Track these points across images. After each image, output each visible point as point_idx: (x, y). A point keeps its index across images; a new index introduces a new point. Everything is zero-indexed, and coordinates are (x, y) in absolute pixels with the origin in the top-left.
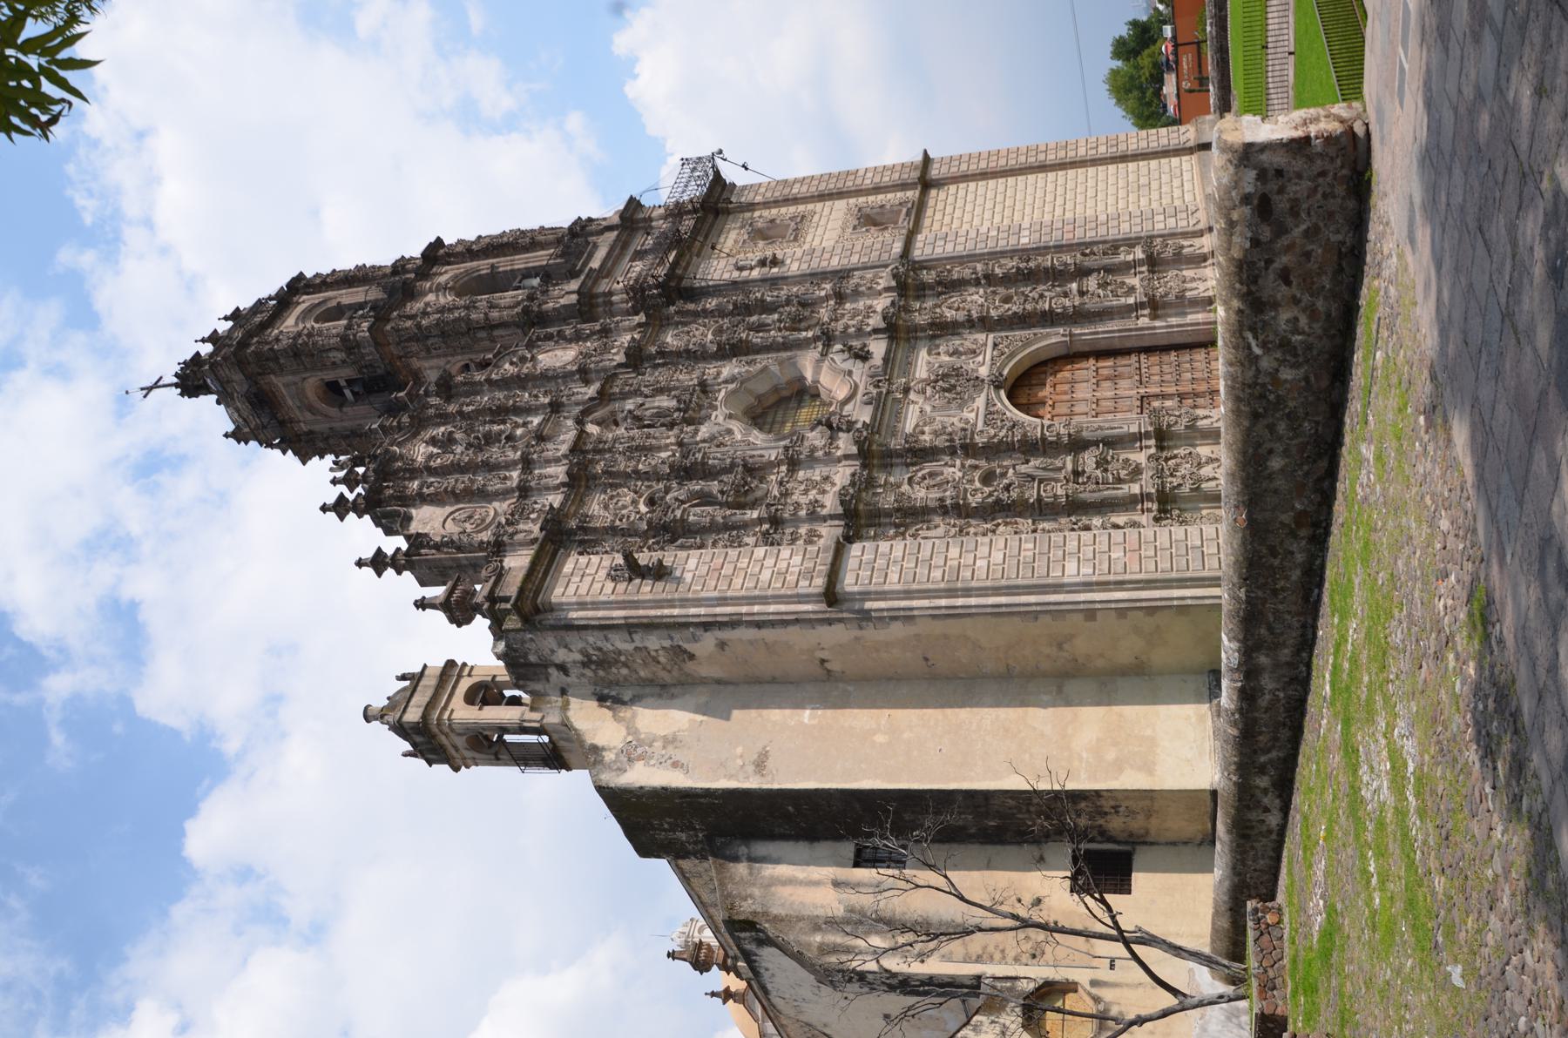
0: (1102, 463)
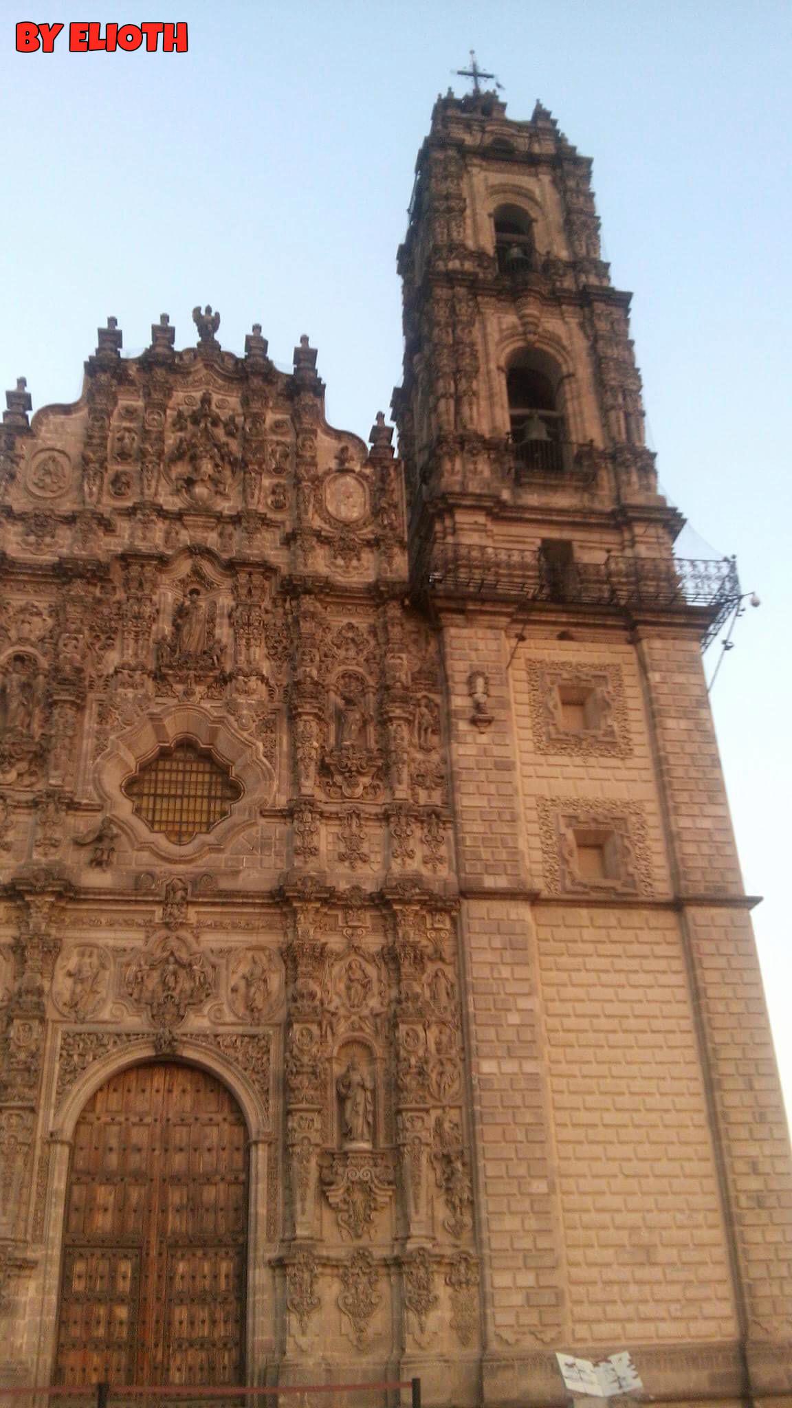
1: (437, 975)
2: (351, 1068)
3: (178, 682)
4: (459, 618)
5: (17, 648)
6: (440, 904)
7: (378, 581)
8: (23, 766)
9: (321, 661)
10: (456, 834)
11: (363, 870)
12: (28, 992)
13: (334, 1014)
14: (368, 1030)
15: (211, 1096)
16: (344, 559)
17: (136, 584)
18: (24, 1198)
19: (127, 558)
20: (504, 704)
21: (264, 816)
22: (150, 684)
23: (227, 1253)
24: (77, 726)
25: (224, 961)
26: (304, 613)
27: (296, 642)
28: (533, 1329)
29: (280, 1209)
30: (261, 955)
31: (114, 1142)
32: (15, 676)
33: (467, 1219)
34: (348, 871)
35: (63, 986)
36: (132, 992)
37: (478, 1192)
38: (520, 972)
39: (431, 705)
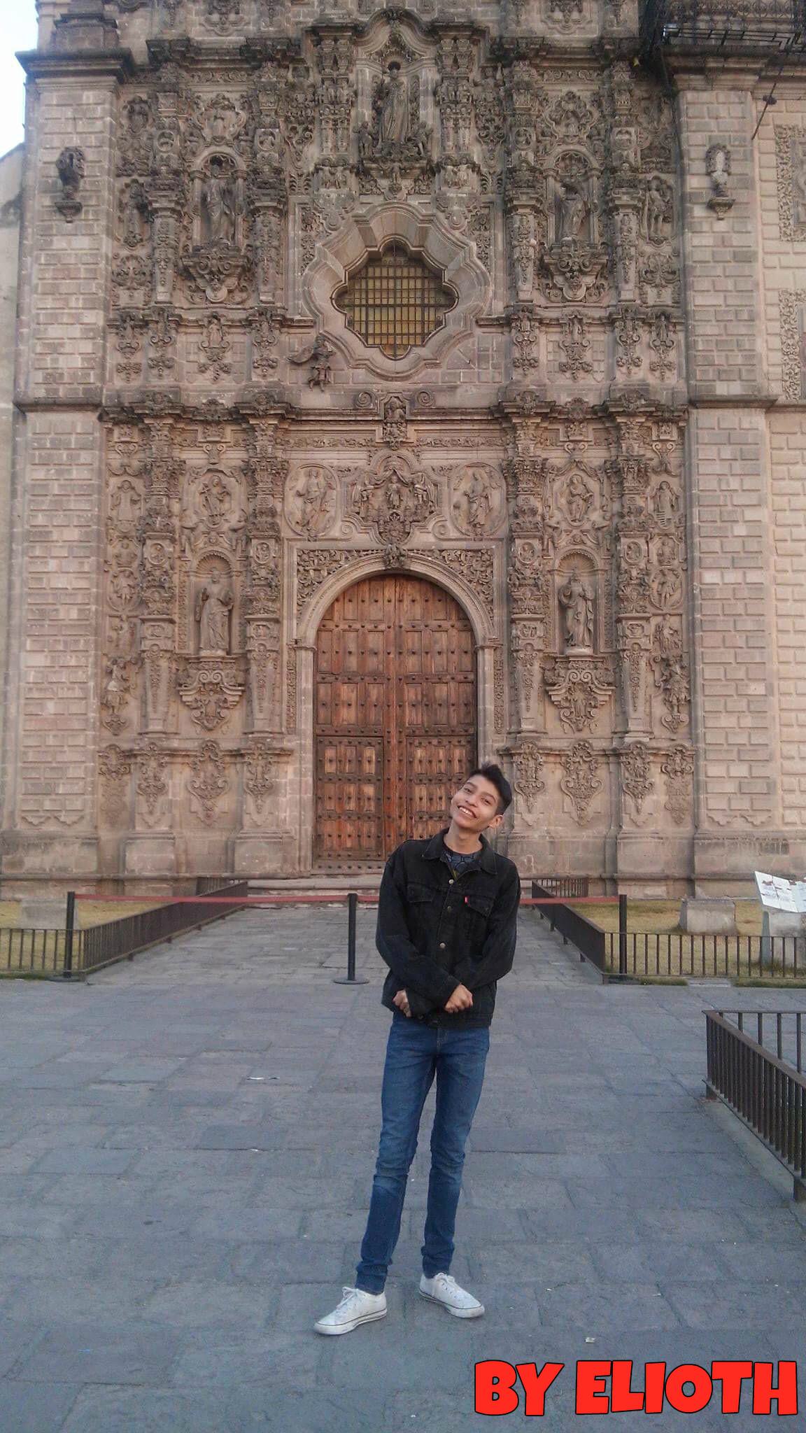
0: (216, 688)
1: (661, 488)
2: (574, 579)
3: (385, 176)
4: (697, 80)
5: (213, 149)
6: (667, 415)
7: (602, 38)
8: (232, 282)
9: (538, 141)
10: (686, 337)
11: (586, 380)
12: (262, 513)
13: (555, 528)
14: (589, 543)
15: (439, 605)
16: (563, 11)
17: (329, 63)
18: (277, 697)
19: (317, 32)
20: (747, 183)
21: (481, 326)
22: (352, 180)
23: (459, 742)
24: (281, 235)
25: (445, 479)
26: (518, 84)
27: (509, 119)
28: (743, 813)
29: (506, 706)
30: (482, 471)
31: (352, 647)
32: (213, 181)
33: (684, 717)
34: (570, 382)
35: (294, 505)
36: (359, 509)
37: (695, 692)
38: (749, 483)
39: (663, 188)
